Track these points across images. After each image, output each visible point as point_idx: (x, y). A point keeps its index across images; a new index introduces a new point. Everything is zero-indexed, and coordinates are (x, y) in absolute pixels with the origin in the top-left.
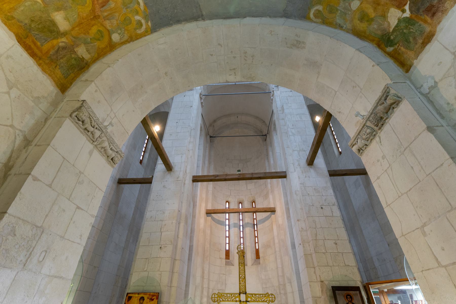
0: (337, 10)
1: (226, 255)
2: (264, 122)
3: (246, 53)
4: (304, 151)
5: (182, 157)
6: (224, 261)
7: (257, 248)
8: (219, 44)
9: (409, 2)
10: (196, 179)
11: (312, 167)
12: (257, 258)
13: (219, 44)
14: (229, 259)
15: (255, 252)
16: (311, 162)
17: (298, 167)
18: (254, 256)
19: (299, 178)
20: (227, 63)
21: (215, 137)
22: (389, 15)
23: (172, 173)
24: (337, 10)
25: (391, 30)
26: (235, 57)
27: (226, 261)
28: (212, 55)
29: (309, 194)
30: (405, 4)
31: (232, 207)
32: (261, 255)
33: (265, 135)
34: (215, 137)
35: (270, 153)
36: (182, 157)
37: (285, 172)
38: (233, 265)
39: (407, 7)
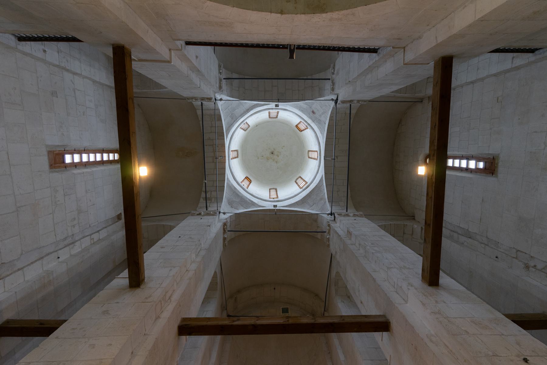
2: (317, 295)
4: (409, 268)
5: (171, 270)
10: (187, 328)
16: (432, 277)
17: (410, 287)
19: (424, 304)
23: (138, 291)
36: (171, 270)
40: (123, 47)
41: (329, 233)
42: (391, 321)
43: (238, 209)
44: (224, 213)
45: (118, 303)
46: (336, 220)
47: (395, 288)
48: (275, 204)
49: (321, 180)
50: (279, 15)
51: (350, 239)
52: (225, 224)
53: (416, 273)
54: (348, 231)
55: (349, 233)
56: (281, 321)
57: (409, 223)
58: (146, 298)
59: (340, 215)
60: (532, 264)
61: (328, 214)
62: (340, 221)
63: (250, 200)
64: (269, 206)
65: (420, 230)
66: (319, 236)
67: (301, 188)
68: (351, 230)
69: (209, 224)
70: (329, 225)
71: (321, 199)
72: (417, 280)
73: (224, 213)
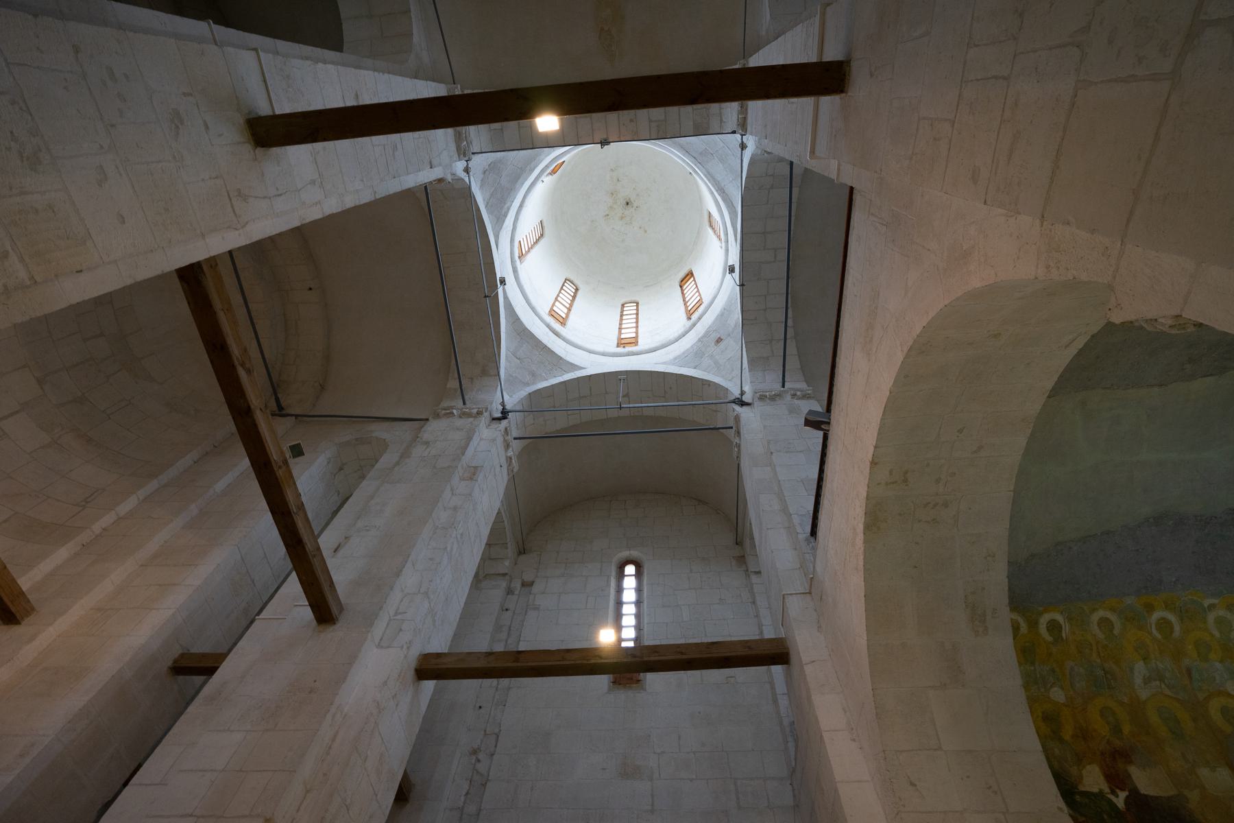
0: (1033, 663)
2: (322, 387)
3: (946, 505)
4: (434, 621)
8: (980, 448)
9: (1126, 793)
13: (980, 448)
16: (430, 669)
19: (385, 683)
20: (928, 465)
22: (1088, 767)
23: (247, 149)
24: (1033, 663)
25: (1082, 788)
26: (938, 481)
28: (960, 431)
30: (1122, 790)
39: (1123, 795)
40: (842, 92)
41: (464, 415)
42: (338, 625)
43: (481, 187)
44: (467, 170)
45: (207, 127)
46: (495, 425)
47: (396, 614)
48: (510, 280)
49: (574, 367)
50: (870, 457)
51: (462, 479)
52: (440, 180)
54: (476, 468)
55: (473, 473)
56: (275, 456)
57: (511, 550)
58: (239, 190)
60: (481, 756)
61: (503, 404)
62: (494, 440)
63: (509, 209)
64: (502, 266)
65: (502, 572)
66: (453, 384)
67: (552, 313)
68: (480, 477)
69: (435, 162)
70: (479, 413)
71: (533, 375)
73: (467, 170)
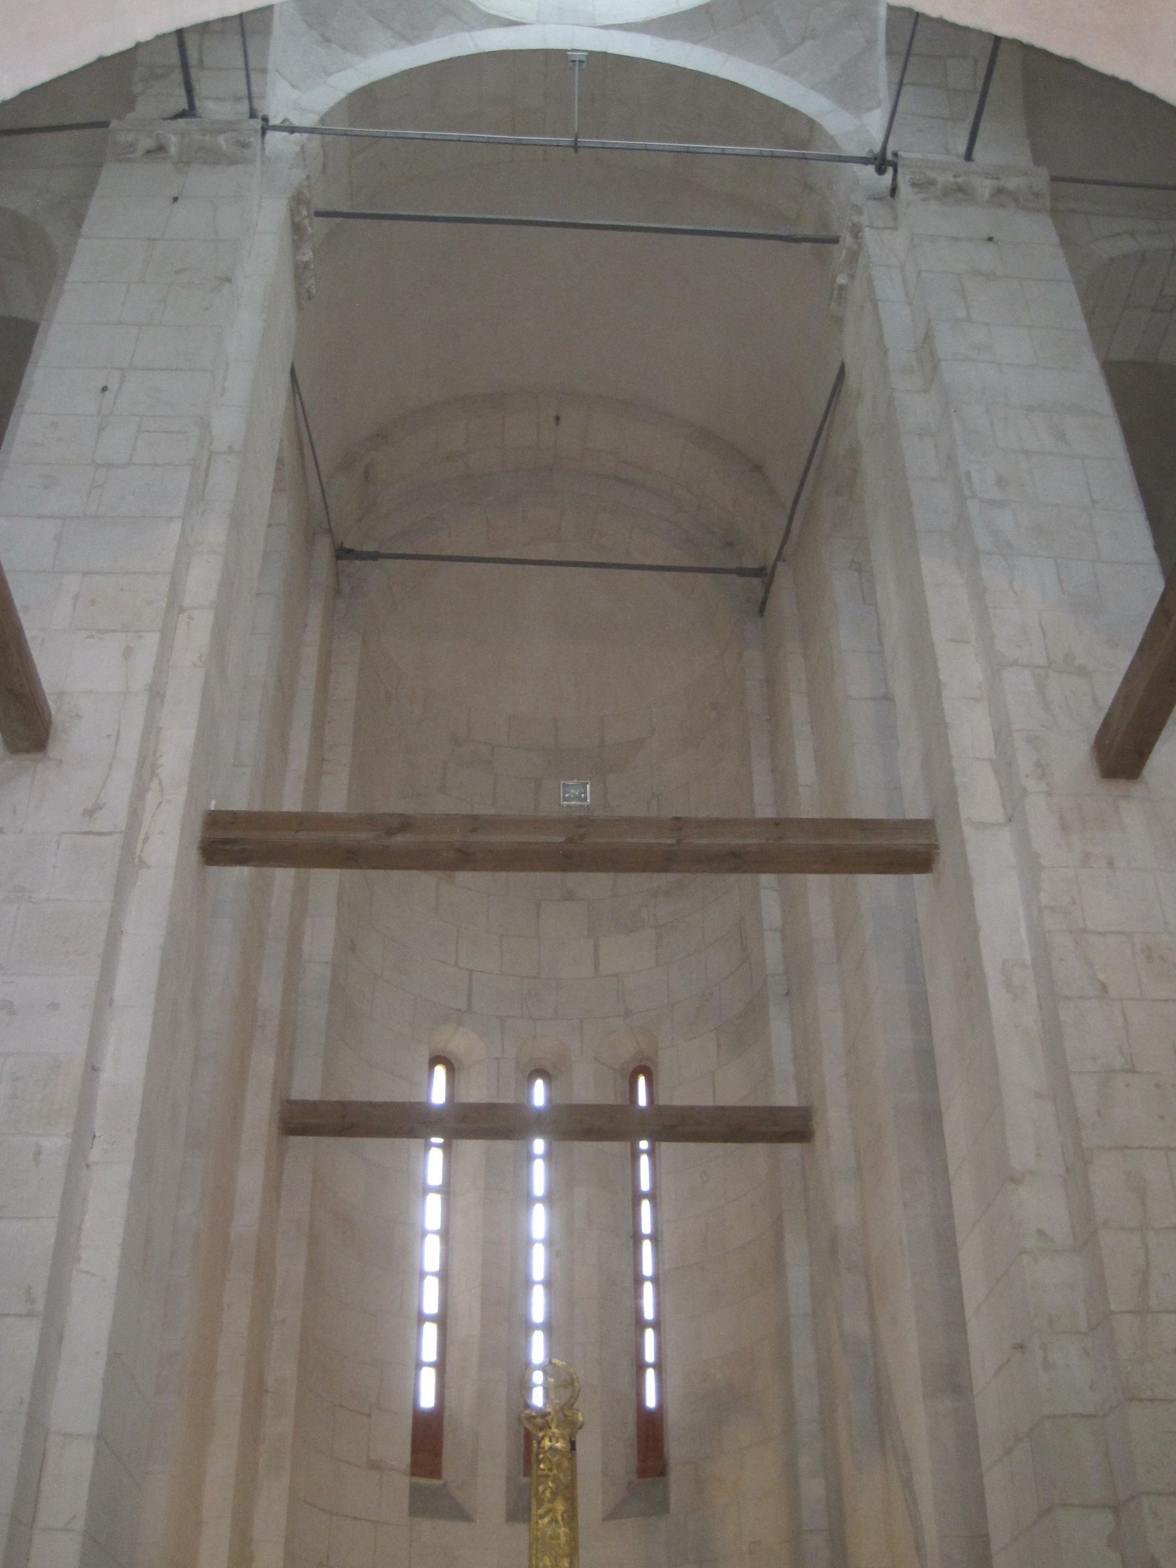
1: (416, 1448)
4: (1082, 672)
5: (128, 652)
6: (400, 1484)
7: (651, 1402)
11: (1137, 789)
12: (642, 1473)
14: (436, 1473)
15: (631, 1429)
18: (625, 1458)
21: (374, 556)
27: (415, 1491)
29: (1104, 988)
31: (477, 1093)
32: (675, 1450)
33: (759, 572)
34: (374, 556)
35: (798, 707)
36: (128, 652)
37: (926, 826)
38: (467, 1517)
53: (1095, 700)
59: (922, 185)
72: (1074, 749)
